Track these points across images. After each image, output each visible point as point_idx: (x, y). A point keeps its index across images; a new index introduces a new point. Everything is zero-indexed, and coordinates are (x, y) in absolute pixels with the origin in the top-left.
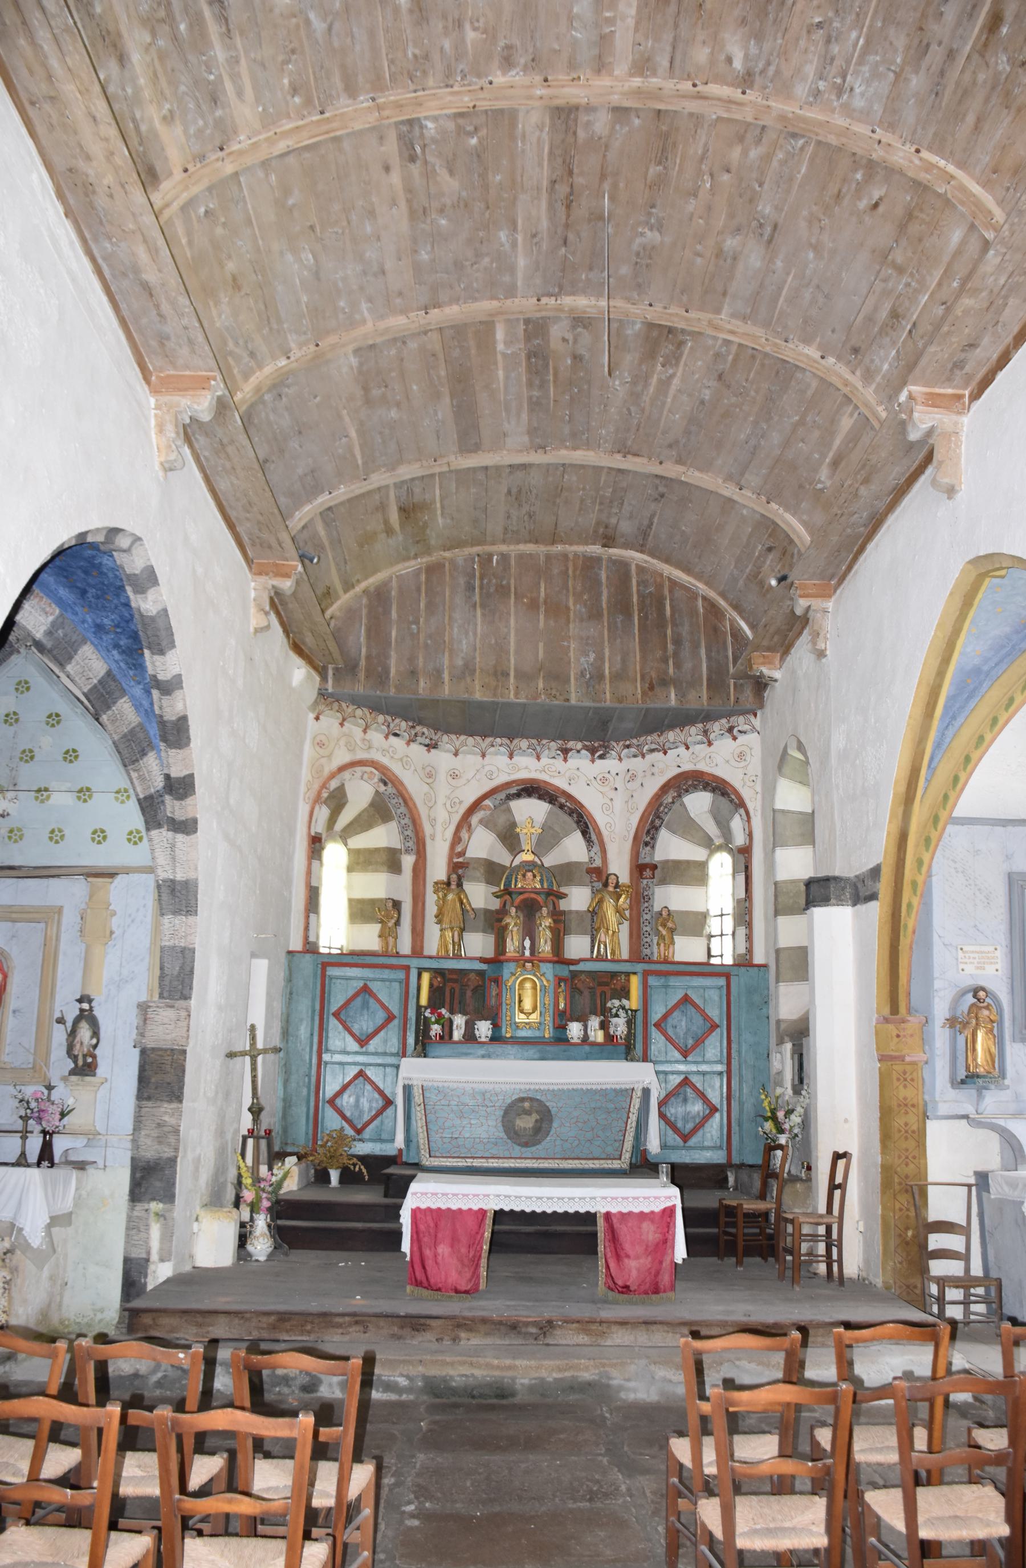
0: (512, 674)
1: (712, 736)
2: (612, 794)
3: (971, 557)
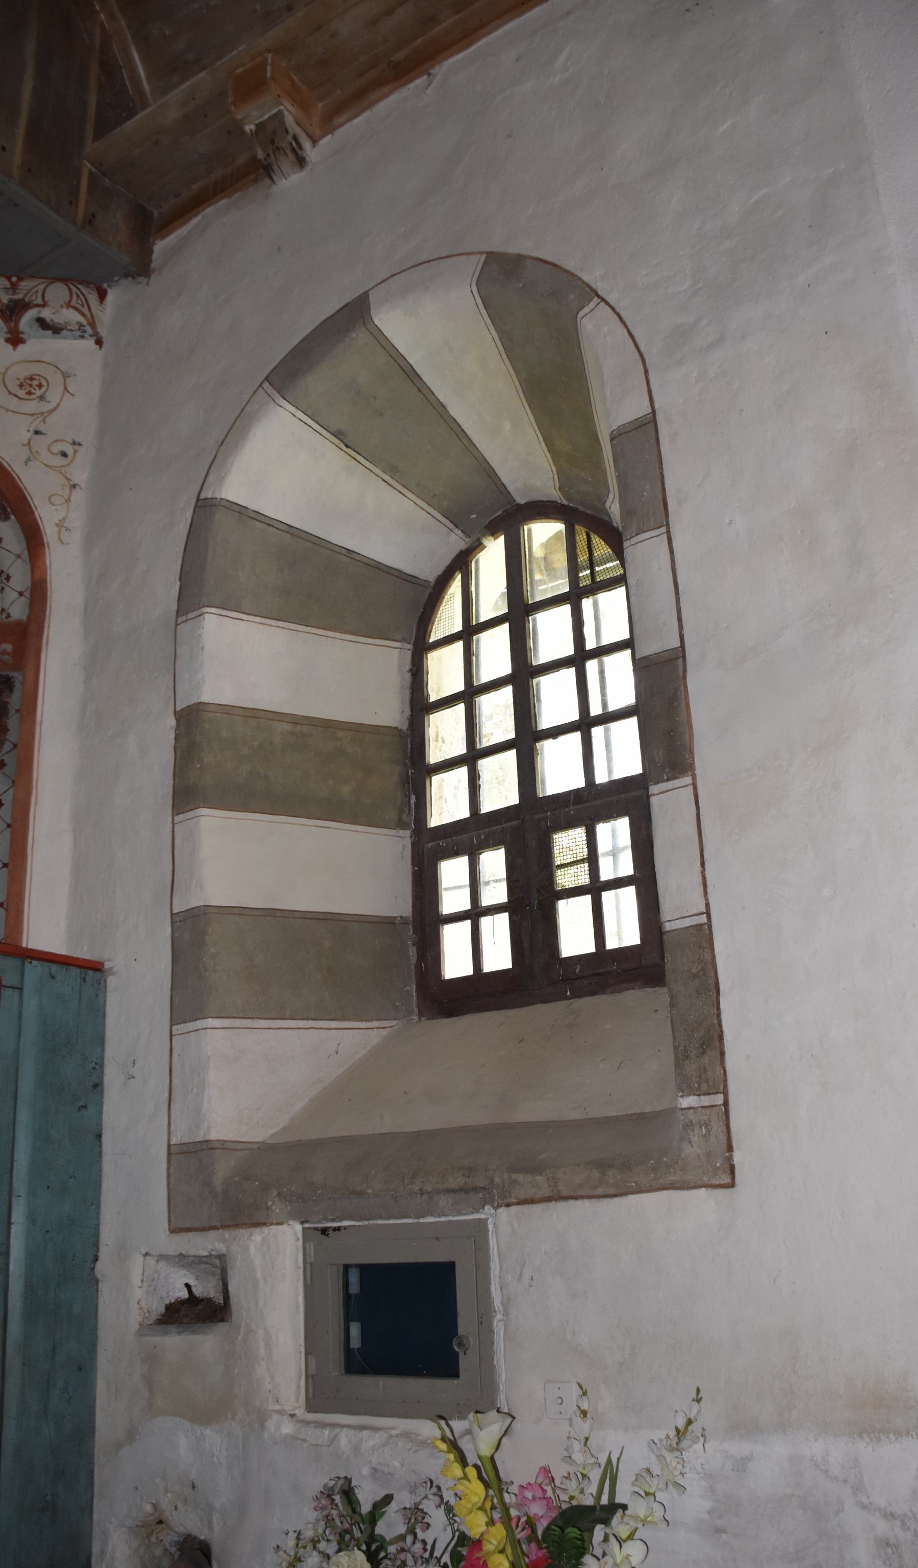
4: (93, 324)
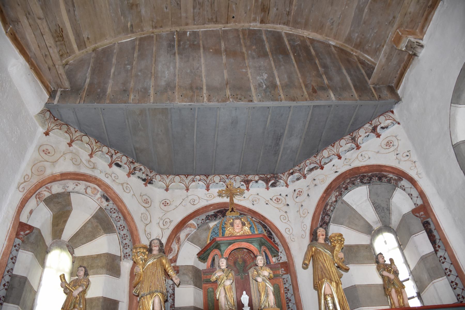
0: (205, 88)
2: (286, 208)
4: (395, 120)
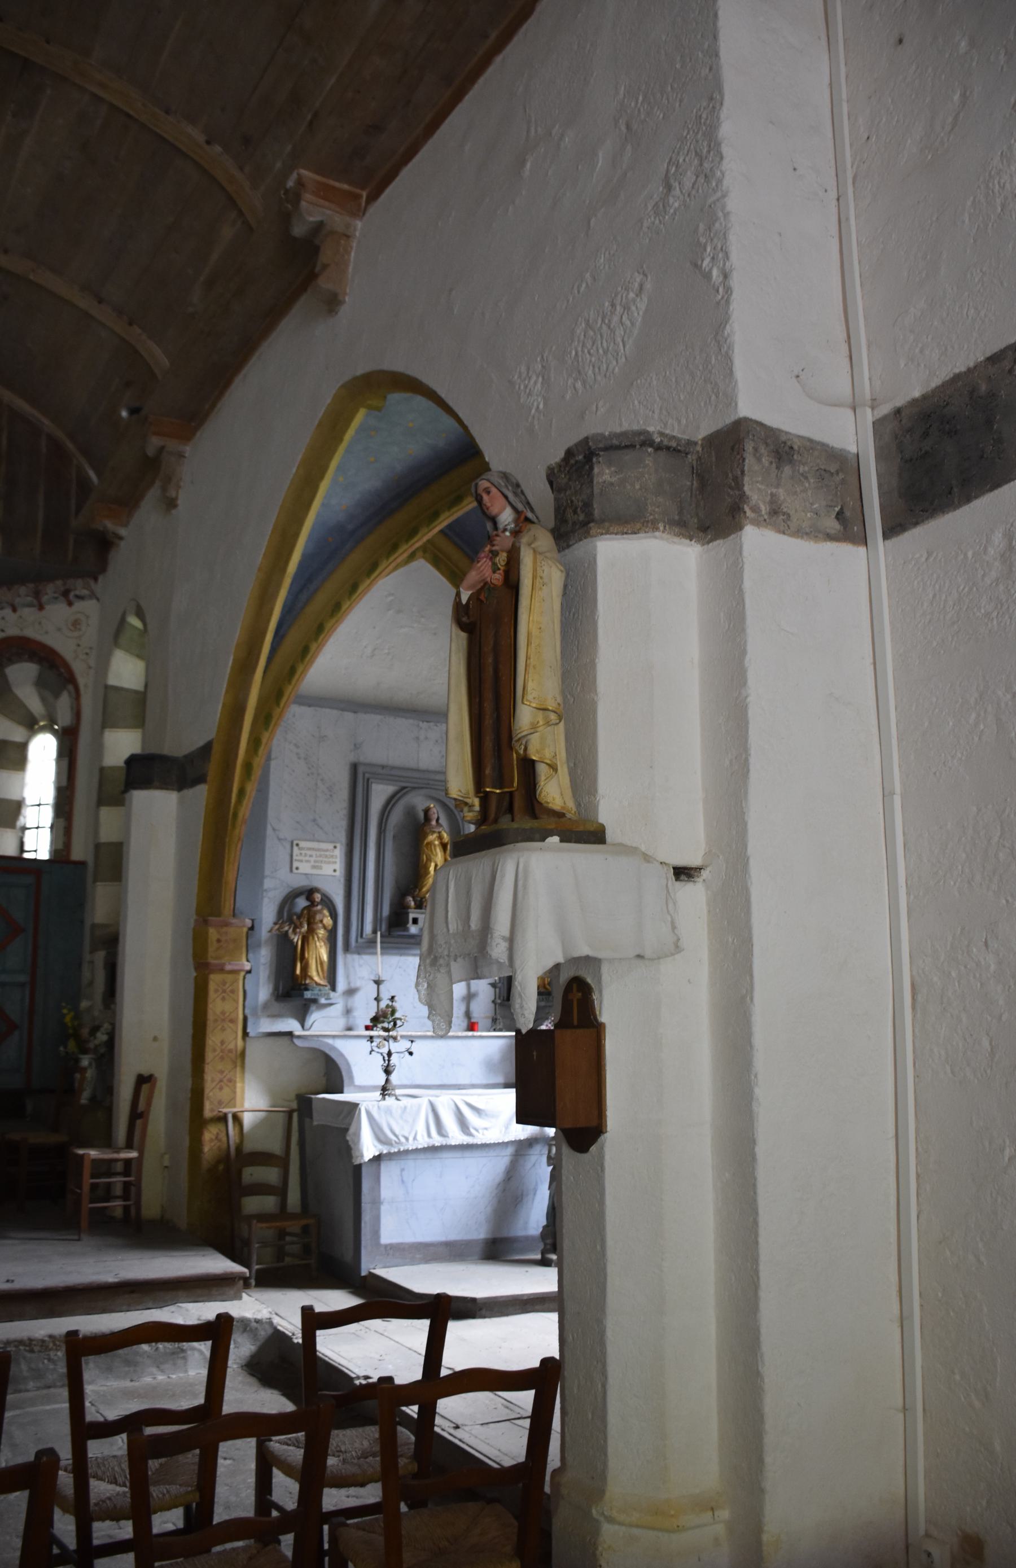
1: (45, 599)
3: (347, 377)
